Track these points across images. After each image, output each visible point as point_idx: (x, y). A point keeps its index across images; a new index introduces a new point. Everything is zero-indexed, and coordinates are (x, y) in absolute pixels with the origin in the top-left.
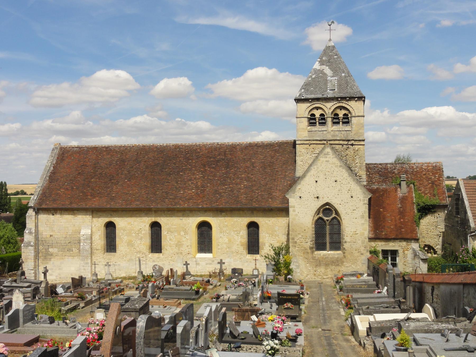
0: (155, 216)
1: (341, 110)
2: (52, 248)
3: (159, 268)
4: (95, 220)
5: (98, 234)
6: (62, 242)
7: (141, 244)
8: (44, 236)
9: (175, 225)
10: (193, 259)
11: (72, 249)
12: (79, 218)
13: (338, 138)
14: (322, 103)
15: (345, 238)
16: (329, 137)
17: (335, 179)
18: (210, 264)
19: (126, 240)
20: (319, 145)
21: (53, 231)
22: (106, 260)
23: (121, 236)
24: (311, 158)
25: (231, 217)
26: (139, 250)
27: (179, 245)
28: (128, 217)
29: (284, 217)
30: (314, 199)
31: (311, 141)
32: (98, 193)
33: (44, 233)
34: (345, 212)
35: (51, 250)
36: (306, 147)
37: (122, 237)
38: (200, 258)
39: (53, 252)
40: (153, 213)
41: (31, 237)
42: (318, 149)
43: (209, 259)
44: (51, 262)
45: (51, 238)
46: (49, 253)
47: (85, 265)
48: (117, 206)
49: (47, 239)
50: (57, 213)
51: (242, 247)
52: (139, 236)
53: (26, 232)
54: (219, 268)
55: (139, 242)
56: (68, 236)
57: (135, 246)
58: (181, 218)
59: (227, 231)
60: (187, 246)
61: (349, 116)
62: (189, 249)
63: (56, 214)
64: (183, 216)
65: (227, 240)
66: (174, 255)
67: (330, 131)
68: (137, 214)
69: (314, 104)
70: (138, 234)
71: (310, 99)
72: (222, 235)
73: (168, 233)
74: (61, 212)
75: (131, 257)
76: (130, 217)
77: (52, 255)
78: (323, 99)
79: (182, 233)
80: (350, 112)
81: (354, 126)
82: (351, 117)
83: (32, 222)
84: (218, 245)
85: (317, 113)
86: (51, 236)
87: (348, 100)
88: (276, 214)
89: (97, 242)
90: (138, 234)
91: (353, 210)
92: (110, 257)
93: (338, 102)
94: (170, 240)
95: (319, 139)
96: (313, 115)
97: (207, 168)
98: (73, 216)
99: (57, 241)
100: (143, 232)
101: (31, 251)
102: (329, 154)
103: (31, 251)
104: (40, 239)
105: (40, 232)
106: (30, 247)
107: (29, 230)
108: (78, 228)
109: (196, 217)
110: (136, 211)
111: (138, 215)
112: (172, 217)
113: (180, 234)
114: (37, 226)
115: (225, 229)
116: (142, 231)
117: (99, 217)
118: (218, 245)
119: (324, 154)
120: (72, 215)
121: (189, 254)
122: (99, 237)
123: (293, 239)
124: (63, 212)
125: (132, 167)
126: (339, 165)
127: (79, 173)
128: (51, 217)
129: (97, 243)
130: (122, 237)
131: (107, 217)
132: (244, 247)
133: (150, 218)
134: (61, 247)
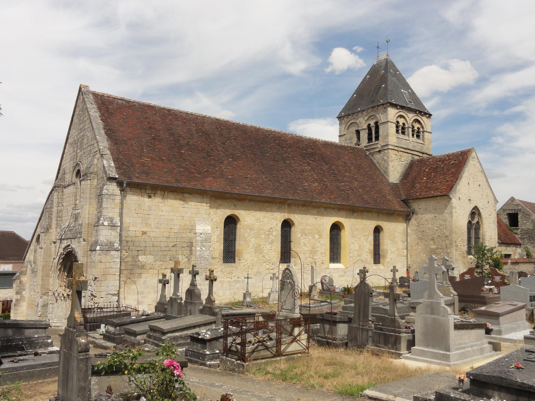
0: (289, 212)
1: (416, 123)
2: (144, 254)
3: (329, 280)
4: (212, 211)
5: (216, 233)
6: (162, 245)
7: (271, 251)
8: (131, 234)
9: (309, 226)
10: (327, 270)
11: (177, 256)
12: (190, 207)
13: (417, 150)
14: (406, 113)
15: (486, 242)
16: (411, 147)
17: (478, 183)
18: (343, 276)
19: (253, 244)
20: (405, 153)
21: (147, 225)
22: (225, 274)
23: (247, 237)
24: (399, 165)
25: (362, 219)
26: (268, 258)
27: (313, 252)
28: (257, 210)
29: (402, 222)
30: (467, 201)
31: (399, 148)
32: (206, 171)
33: (131, 229)
34: (485, 216)
35: (141, 258)
36: (396, 153)
37: (248, 239)
38: (333, 269)
39: (145, 262)
40: (287, 207)
41: (113, 234)
42: (404, 157)
43: (342, 270)
44: (142, 280)
45: (143, 236)
46: (138, 263)
47: (202, 283)
48: (248, 192)
49: (137, 239)
50: (156, 195)
51: (370, 255)
52: (269, 238)
53: (103, 223)
54: (392, 277)
55: (268, 247)
56: (172, 235)
57: (264, 253)
58: (316, 217)
59: (358, 236)
60: (322, 254)
61: (421, 130)
62: (323, 257)
63: (155, 197)
64: (318, 214)
65: (357, 248)
66: (308, 265)
67: (411, 141)
68: (268, 207)
69: (400, 112)
70: (268, 235)
71: (399, 105)
72: (353, 241)
73: (302, 236)
74: (163, 193)
75: (259, 268)
76: (259, 211)
77: (143, 267)
78: (406, 108)
79: (317, 236)
80: (423, 127)
81: (426, 141)
82: (423, 132)
83: (113, 206)
84: (350, 253)
85: (401, 121)
86: (144, 233)
87: (422, 116)
88: (396, 219)
89: (213, 247)
90: (268, 235)
91: (490, 215)
92: (231, 269)
93: (416, 115)
94: (305, 245)
95: (405, 147)
96: (398, 122)
97: (308, 160)
98: (181, 202)
99: (154, 243)
100: (274, 233)
101: (114, 260)
102: (475, 159)
103: (114, 260)
104: (124, 238)
105: (124, 225)
106: (113, 253)
107: (108, 219)
108: (188, 223)
109: (331, 216)
110: (267, 202)
111: (268, 209)
112: (306, 214)
113: (314, 238)
114: (121, 215)
115: (356, 233)
116: (273, 231)
117: (218, 208)
118: (350, 253)
119: (472, 157)
120: (180, 200)
121: (322, 263)
122: (217, 237)
123: (456, 242)
124: (166, 193)
125: (224, 143)
126: (481, 170)
127: (154, 138)
128: (146, 201)
129: (214, 248)
130: (248, 239)
131: (229, 208)
132: (371, 255)
133: (283, 214)
134: (160, 253)
